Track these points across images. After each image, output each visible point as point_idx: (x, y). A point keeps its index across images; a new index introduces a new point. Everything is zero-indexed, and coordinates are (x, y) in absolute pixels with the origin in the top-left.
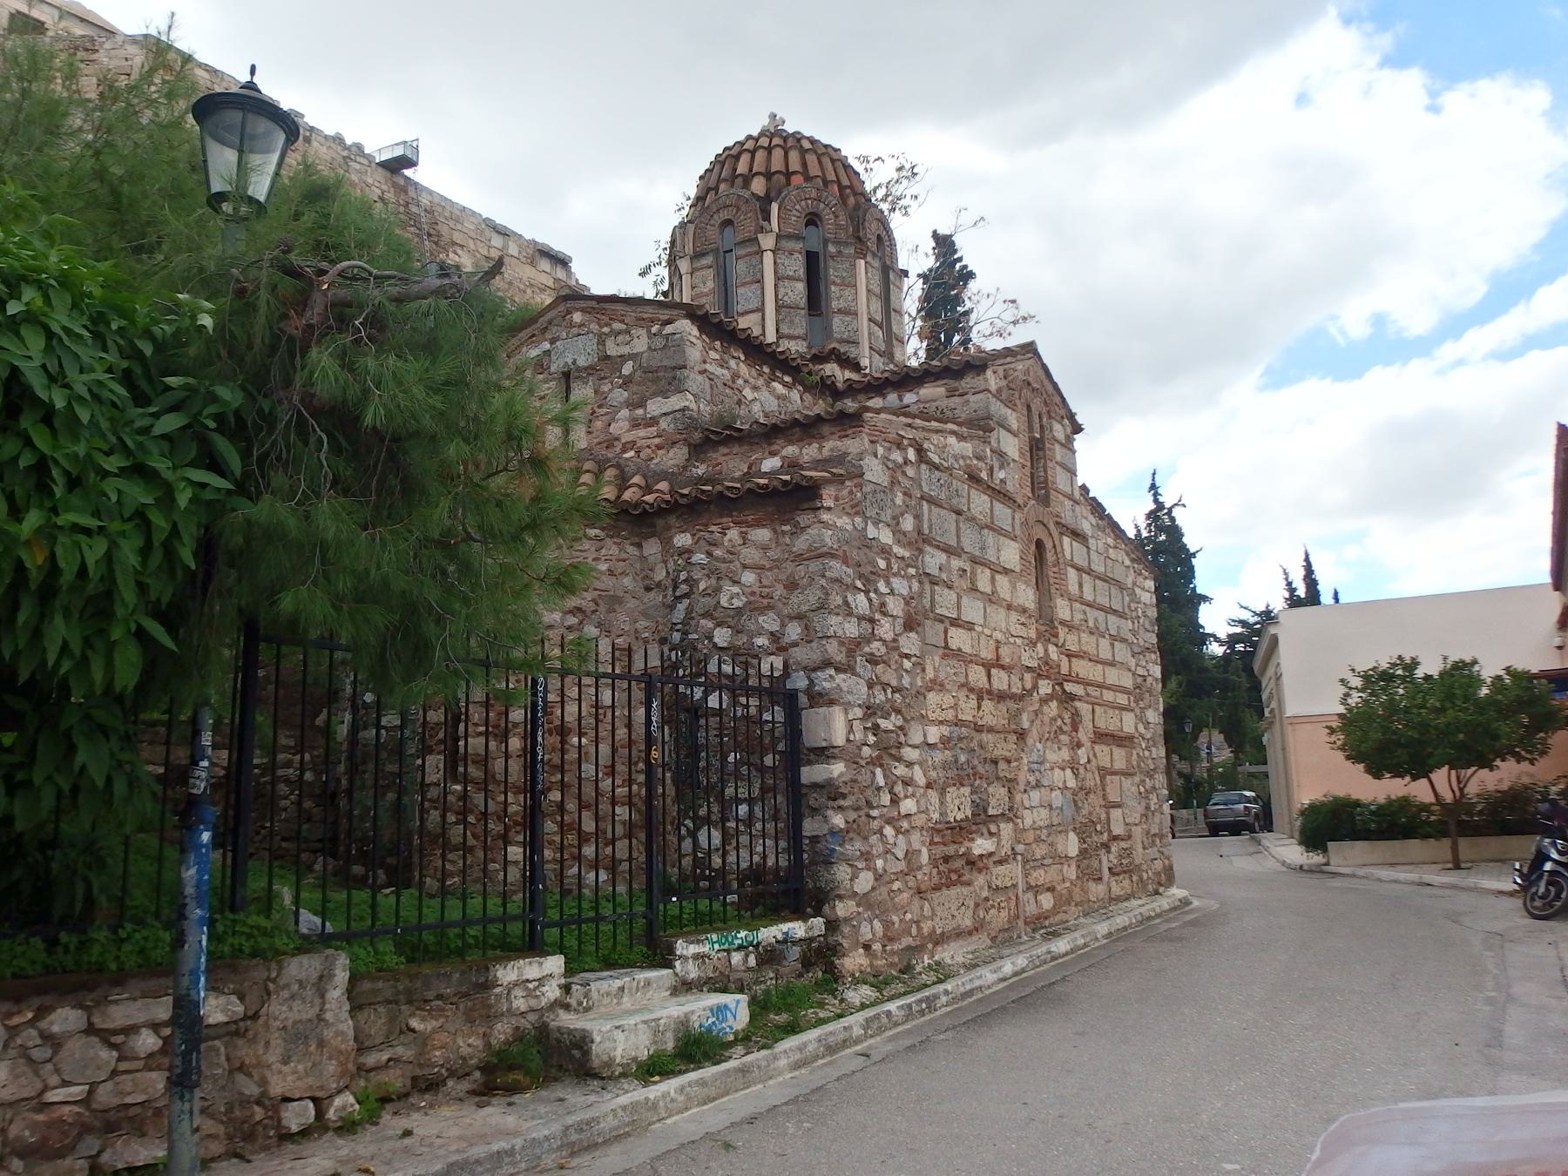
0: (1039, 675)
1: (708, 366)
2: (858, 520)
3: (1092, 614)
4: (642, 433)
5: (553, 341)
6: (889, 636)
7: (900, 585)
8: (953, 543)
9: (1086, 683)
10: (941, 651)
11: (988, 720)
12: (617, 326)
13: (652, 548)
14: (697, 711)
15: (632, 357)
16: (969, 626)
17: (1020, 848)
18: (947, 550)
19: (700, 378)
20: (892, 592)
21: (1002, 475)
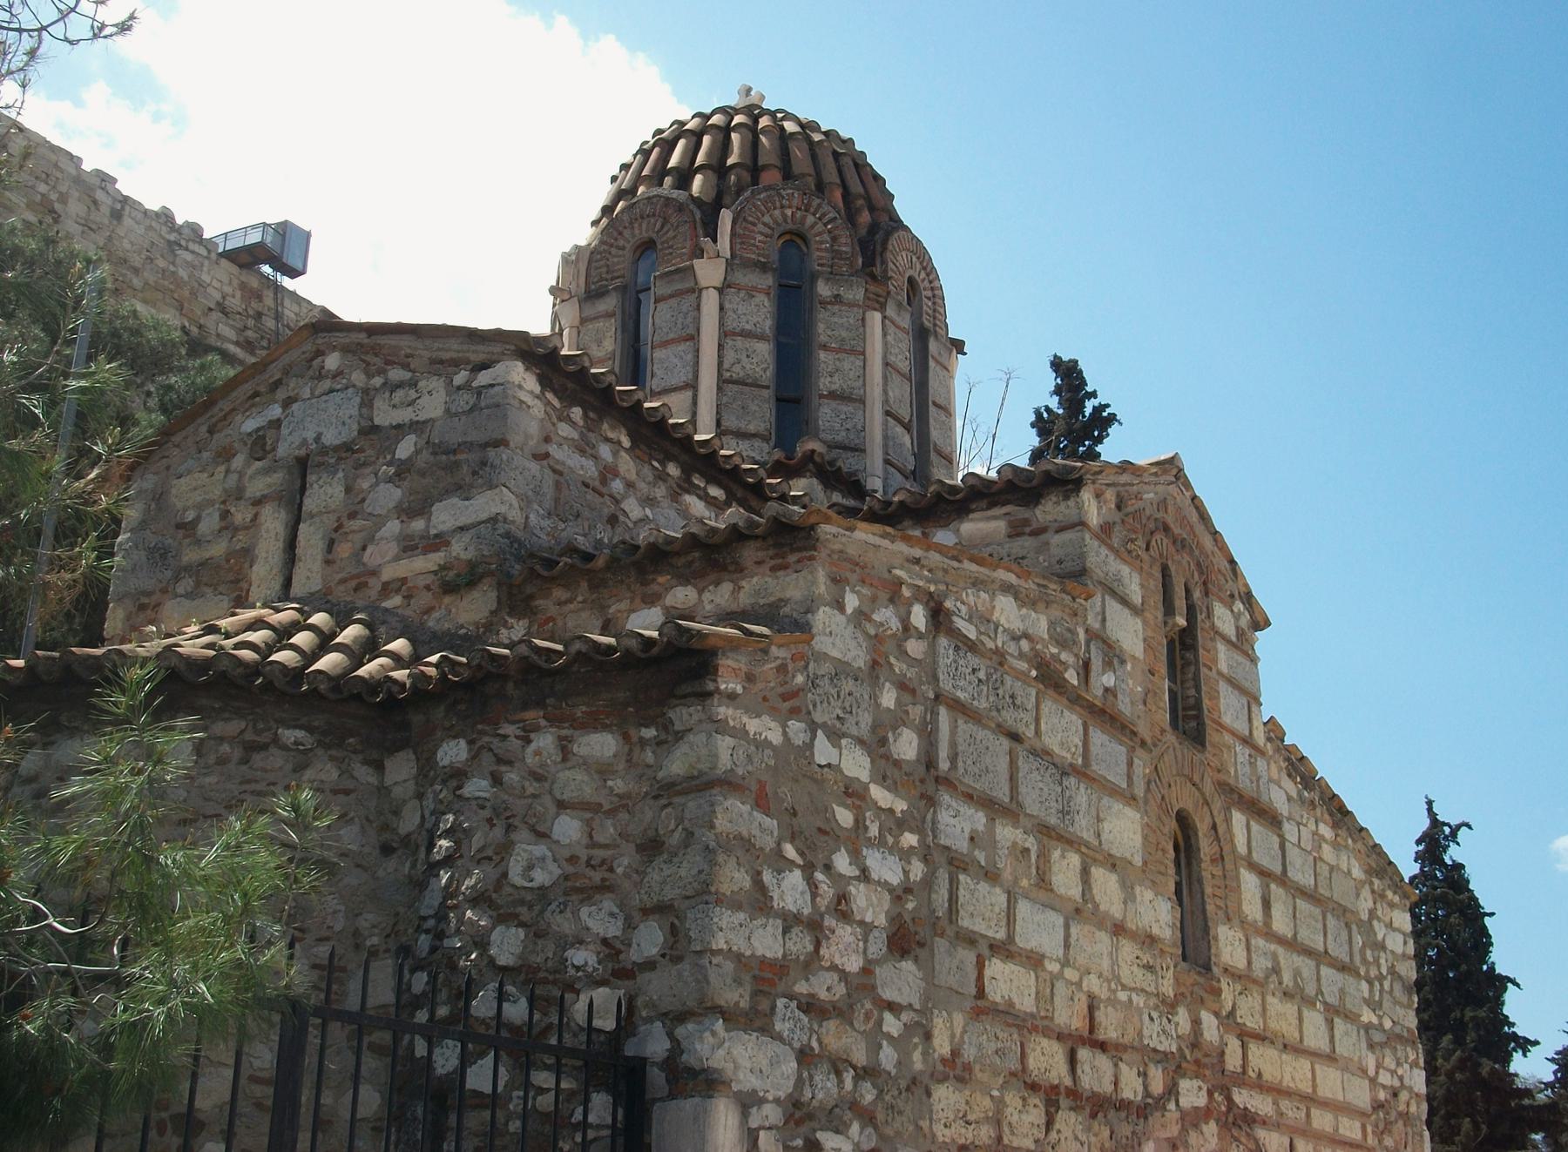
0: (1176, 1067)
1: (552, 449)
2: (795, 726)
3: (1290, 962)
6: (853, 964)
7: (886, 869)
8: (1002, 793)
9: (1277, 1091)
10: (969, 1004)
12: (396, 374)
13: (401, 769)
14: (446, 1096)
15: (416, 426)
16: (1034, 961)
18: (988, 804)
19: (534, 466)
20: (864, 875)
21: (1109, 680)
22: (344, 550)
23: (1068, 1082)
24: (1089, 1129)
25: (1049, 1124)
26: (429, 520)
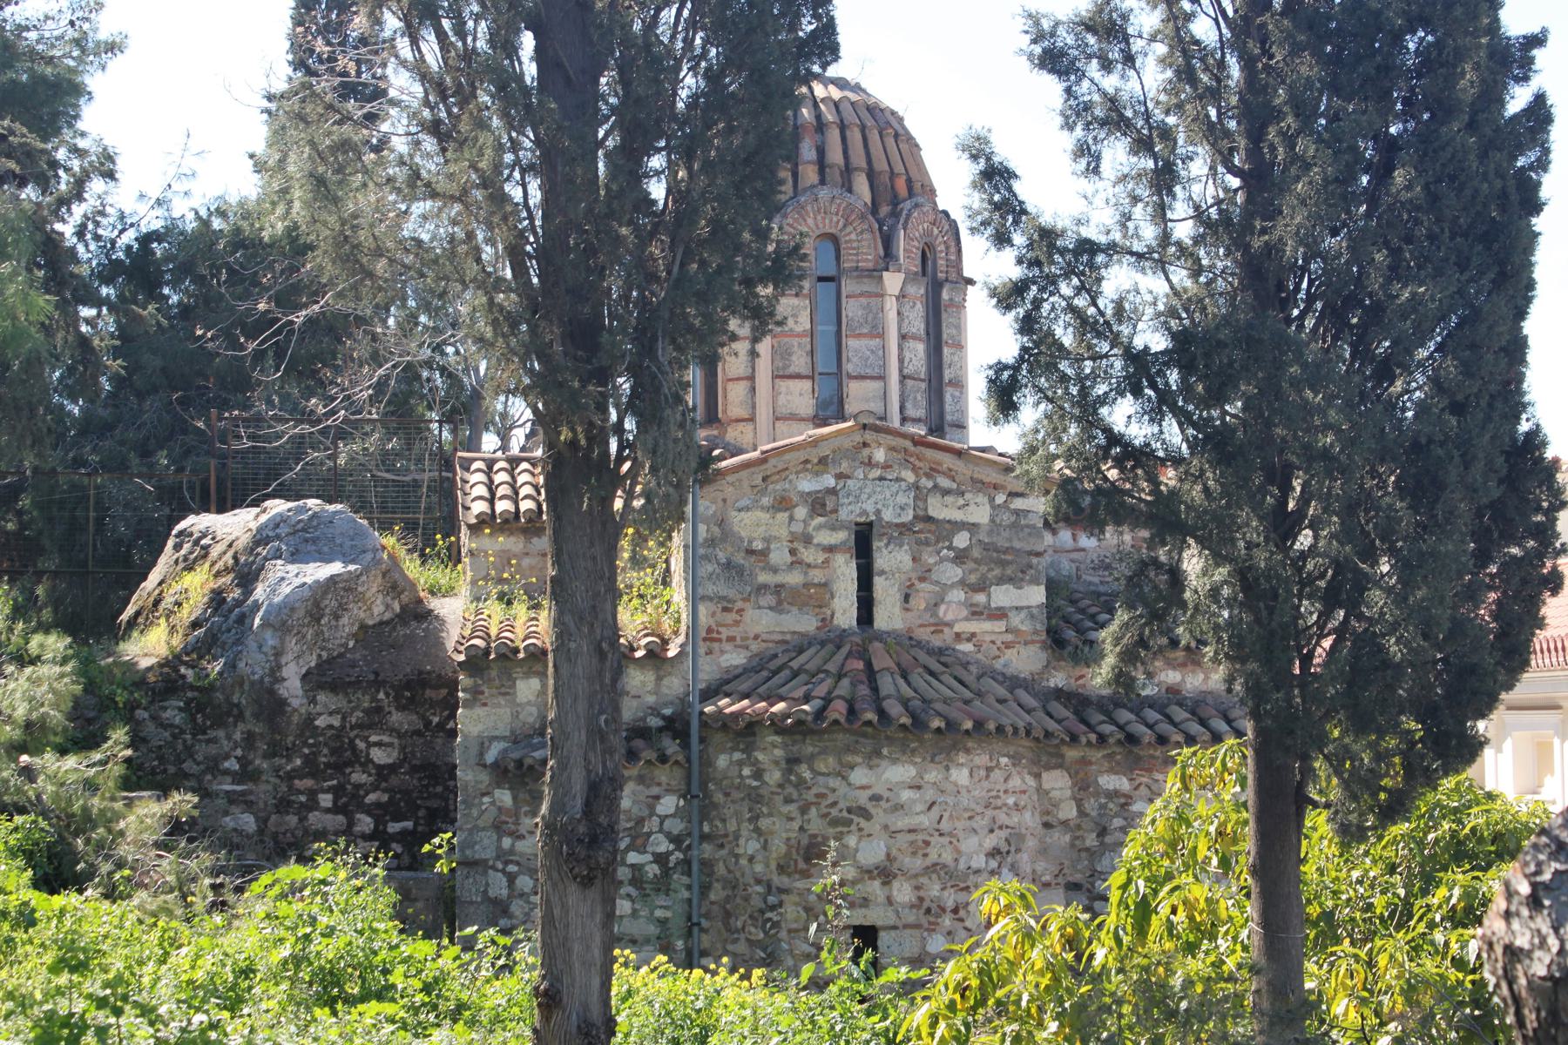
4: (987, 626)
5: (839, 476)
12: (944, 482)
15: (972, 527)
22: (919, 603)
26: (989, 595)
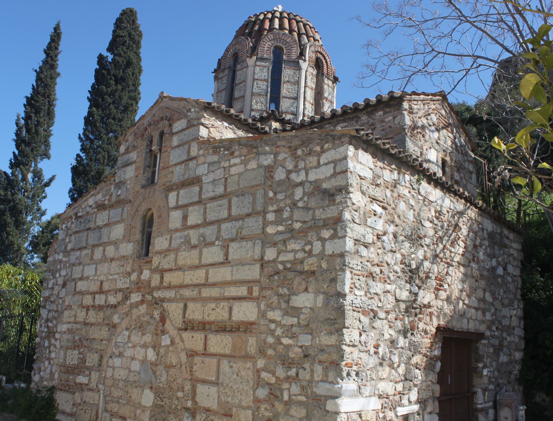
11: (91, 320)
17: (101, 386)
23: (92, 304)
24: (97, 314)
25: (87, 315)
